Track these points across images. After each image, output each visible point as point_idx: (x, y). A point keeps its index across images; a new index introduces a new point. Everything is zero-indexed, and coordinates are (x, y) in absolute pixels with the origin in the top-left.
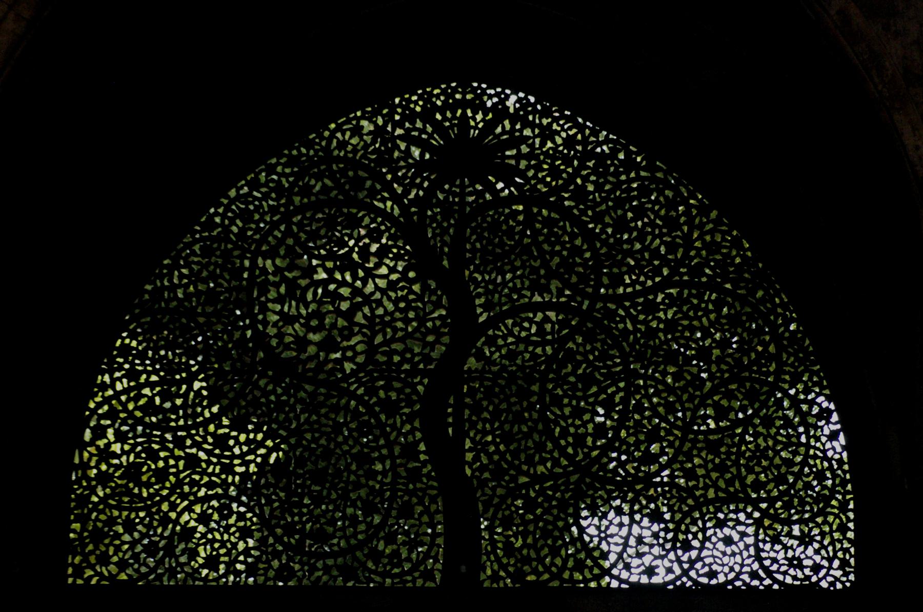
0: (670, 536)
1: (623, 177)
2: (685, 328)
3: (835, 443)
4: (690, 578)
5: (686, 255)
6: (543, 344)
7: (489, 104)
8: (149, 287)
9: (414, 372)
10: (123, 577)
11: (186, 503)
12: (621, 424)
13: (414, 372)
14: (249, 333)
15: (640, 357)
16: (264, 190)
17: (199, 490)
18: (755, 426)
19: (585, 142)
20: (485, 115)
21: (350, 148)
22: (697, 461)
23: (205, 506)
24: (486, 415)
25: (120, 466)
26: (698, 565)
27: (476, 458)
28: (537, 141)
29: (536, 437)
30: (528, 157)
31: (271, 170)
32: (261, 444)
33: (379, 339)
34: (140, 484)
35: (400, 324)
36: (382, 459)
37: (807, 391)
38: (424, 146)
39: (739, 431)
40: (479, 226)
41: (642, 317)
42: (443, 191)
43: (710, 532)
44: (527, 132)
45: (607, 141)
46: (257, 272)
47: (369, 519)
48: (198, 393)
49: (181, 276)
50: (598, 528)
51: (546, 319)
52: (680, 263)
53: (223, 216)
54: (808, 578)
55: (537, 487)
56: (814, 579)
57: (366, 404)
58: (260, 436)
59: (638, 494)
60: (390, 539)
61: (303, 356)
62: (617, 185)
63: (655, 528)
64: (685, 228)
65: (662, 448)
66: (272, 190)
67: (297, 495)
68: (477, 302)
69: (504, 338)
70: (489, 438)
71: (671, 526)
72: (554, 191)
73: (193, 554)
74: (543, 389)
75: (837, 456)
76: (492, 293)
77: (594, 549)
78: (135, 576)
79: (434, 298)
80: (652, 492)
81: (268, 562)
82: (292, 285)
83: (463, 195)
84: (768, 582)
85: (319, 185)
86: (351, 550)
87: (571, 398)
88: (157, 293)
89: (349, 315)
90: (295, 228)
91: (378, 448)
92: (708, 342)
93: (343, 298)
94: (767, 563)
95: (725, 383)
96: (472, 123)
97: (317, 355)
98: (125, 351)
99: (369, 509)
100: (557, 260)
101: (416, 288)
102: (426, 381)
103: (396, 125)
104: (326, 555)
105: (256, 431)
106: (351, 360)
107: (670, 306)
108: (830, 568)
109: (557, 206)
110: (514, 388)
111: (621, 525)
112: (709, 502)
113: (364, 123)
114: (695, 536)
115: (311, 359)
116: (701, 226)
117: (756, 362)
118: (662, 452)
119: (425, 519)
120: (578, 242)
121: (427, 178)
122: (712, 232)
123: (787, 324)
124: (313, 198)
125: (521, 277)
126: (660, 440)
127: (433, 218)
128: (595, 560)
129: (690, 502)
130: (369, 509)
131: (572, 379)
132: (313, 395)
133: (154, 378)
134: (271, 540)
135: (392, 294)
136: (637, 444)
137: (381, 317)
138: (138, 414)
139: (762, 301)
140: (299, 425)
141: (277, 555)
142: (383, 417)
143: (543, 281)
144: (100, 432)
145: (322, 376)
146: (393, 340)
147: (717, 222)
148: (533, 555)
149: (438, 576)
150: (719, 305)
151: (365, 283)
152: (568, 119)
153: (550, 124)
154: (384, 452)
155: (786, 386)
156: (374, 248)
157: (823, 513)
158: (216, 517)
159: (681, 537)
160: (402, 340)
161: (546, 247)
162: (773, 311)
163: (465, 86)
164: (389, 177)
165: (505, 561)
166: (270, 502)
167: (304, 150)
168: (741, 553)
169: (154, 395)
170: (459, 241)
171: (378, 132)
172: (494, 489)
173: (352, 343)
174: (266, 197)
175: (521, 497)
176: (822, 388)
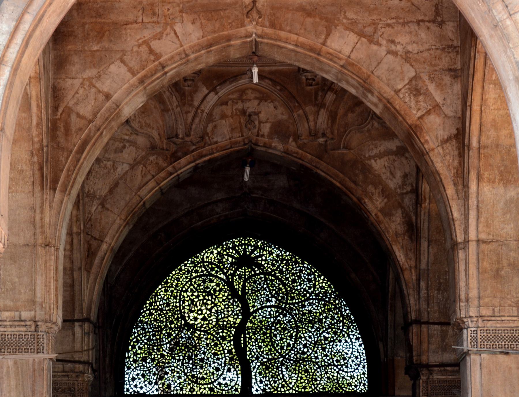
0: (311, 377)
1: (294, 266)
2: (314, 312)
3: (361, 347)
4: (317, 390)
5: (314, 290)
6: (271, 318)
7: (253, 244)
8: (148, 302)
9: (230, 327)
10: (141, 392)
14: (179, 316)
15: (301, 322)
16: (184, 271)
19: (282, 255)
20: (251, 247)
21: (210, 258)
22: (319, 354)
24: (253, 340)
26: (319, 386)
27: (251, 354)
28: (268, 255)
29: (269, 347)
30: (266, 260)
31: (185, 265)
32: (184, 350)
33: (220, 317)
34: (146, 363)
35: (226, 313)
36: (221, 354)
37: (352, 331)
38: (233, 257)
40: (250, 282)
41: (301, 309)
42: (239, 271)
43: (323, 376)
44: (265, 253)
45: (289, 255)
46: (182, 297)
47: (217, 373)
48: (164, 335)
49: (158, 298)
50: (288, 375)
51: (271, 310)
52: (312, 292)
53: (171, 280)
54: (353, 389)
56: (355, 389)
57: (216, 337)
58: (183, 348)
59: (301, 364)
61: (196, 323)
62: (293, 269)
63: (306, 374)
64: (314, 282)
65: (308, 350)
66: (186, 271)
67: (195, 365)
68: (250, 305)
69: (259, 316)
70: (254, 347)
71: (311, 374)
72: (273, 271)
74: (271, 332)
75: (362, 352)
76: (255, 302)
78: (146, 391)
79: (237, 304)
80: (305, 363)
81: (187, 386)
83: (245, 272)
84: (341, 390)
85: (200, 270)
86: (212, 383)
87: (280, 335)
88: (151, 304)
90: (193, 283)
91: (220, 351)
92: (321, 317)
93: (208, 305)
94: (341, 385)
95: (327, 329)
96: (247, 250)
97: (201, 323)
98: (141, 322)
99: (217, 369)
100: (274, 292)
101: (231, 301)
102: (234, 330)
103: (225, 251)
104: (204, 384)
105: (182, 346)
106: (211, 324)
107: (309, 306)
108: (360, 386)
109: (274, 276)
110: (262, 332)
112: (322, 366)
113: (214, 250)
114: (318, 377)
115: (199, 324)
116: (319, 281)
117: (337, 323)
118: (308, 351)
119: (235, 372)
120: (281, 286)
121: (234, 267)
122: (322, 283)
123: (345, 311)
124: (199, 274)
125: (264, 297)
126: (307, 347)
127: (236, 280)
128: (288, 385)
129: (317, 366)
131: (280, 329)
132: (200, 335)
133: (150, 330)
134: (187, 380)
135: (224, 303)
137: (220, 310)
138: (145, 341)
139: (338, 304)
141: (189, 384)
142: (221, 341)
143: (270, 299)
144: (134, 347)
145: (203, 329)
146: (224, 317)
147: (324, 280)
148: (268, 383)
149: (239, 390)
150: (324, 305)
151: (215, 300)
152: (277, 249)
153: (271, 250)
154: (222, 352)
155: (345, 330)
156: (218, 289)
157: (357, 369)
159: (314, 377)
160: (227, 317)
161: (271, 288)
162: (341, 307)
163: (245, 238)
164: (222, 267)
165: (260, 385)
167: (196, 259)
168: (333, 382)
170: (244, 286)
171: (219, 253)
172: (256, 363)
173: (211, 318)
174: (184, 274)
175: (264, 365)
176: (357, 330)
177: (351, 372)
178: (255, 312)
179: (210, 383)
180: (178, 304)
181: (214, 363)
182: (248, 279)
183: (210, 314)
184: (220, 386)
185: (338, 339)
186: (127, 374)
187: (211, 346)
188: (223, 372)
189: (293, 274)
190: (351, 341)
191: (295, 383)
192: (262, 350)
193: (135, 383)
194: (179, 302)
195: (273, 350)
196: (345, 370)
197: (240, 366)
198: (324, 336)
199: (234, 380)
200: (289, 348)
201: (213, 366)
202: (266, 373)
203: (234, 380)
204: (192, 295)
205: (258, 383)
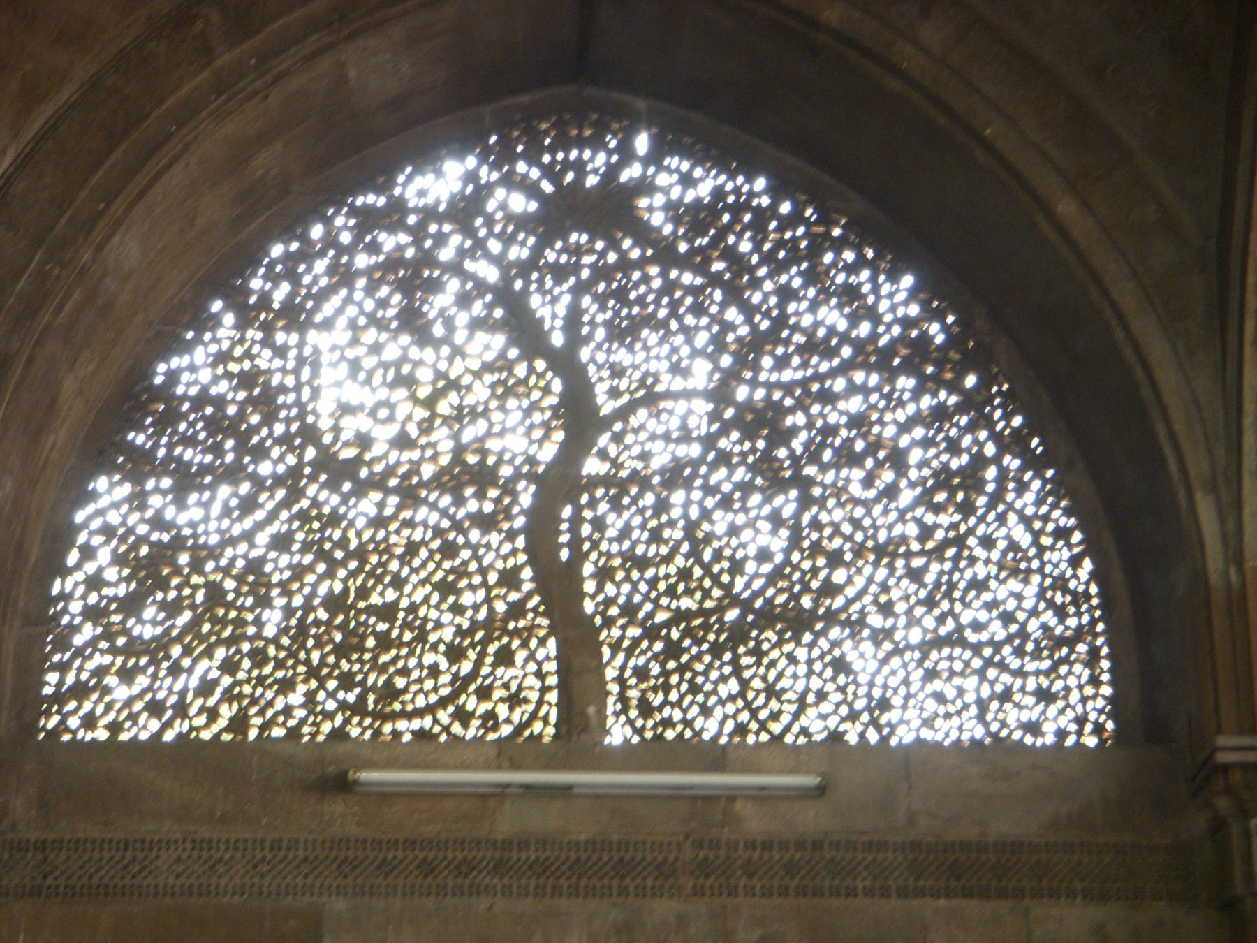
11: (204, 646)
12: (795, 540)
13: (517, 476)
14: (294, 427)
15: (814, 458)
17: (224, 628)
18: (971, 549)
19: (737, 191)
22: (895, 594)
23: (233, 650)
25: (115, 598)
27: (600, 589)
32: (310, 568)
36: (472, 588)
38: (532, 190)
39: (951, 552)
47: (454, 669)
50: (764, 679)
53: (266, 278)
55: (683, 625)
57: (452, 518)
58: (308, 559)
59: (817, 635)
60: (484, 693)
62: (780, 244)
73: (213, 715)
77: (759, 708)
82: (355, 365)
86: (430, 709)
89: (430, 403)
92: (904, 441)
97: (385, 456)
99: (455, 654)
102: (533, 488)
104: (394, 716)
108: (1080, 733)
109: (702, 269)
111: (795, 677)
118: (849, 581)
122: (906, 303)
123: (1007, 417)
126: (848, 565)
130: (455, 654)
132: (381, 505)
136: (815, 571)
140: (362, 545)
144: (88, 553)
147: (913, 294)
158: (246, 664)
166: (319, 645)
169: (165, 505)
171: (472, 177)
176: (1059, 499)
177: (1038, 673)
178: (623, 414)
179: (419, 713)
180: (290, 381)
181: (438, 625)
182: (593, 281)
183: (431, 420)
184: (465, 726)
185: (981, 530)
186: (54, 667)
187: (432, 552)
188: (479, 663)
189: (782, 267)
190: (1036, 542)
191: (796, 716)
192: (650, 573)
193: (87, 706)
194: (296, 372)
195: (698, 572)
196: (1015, 663)
197: (552, 643)
198: (919, 522)
199: (526, 701)
200: (767, 568)
201: (433, 638)
202: (666, 674)
203: (526, 701)
204: (355, 341)
205: (633, 713)
